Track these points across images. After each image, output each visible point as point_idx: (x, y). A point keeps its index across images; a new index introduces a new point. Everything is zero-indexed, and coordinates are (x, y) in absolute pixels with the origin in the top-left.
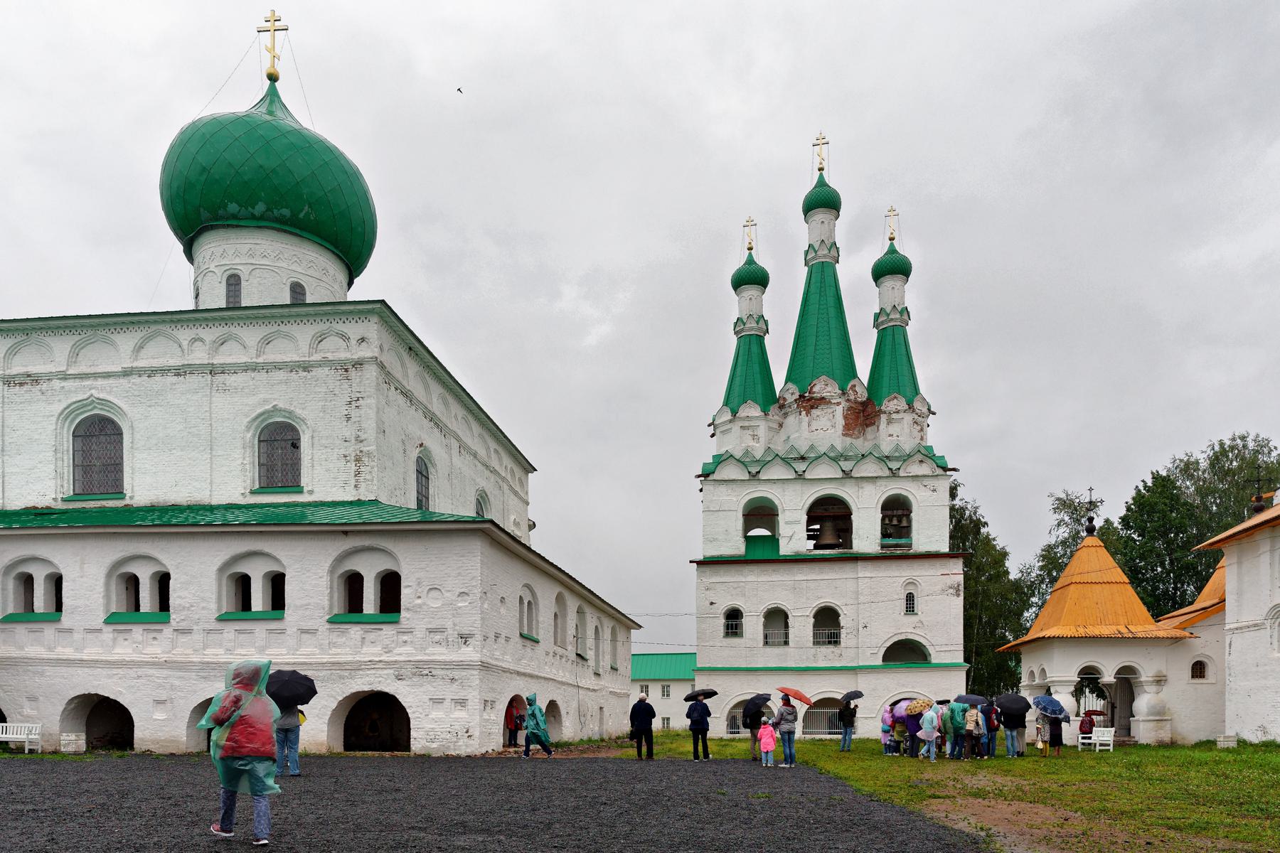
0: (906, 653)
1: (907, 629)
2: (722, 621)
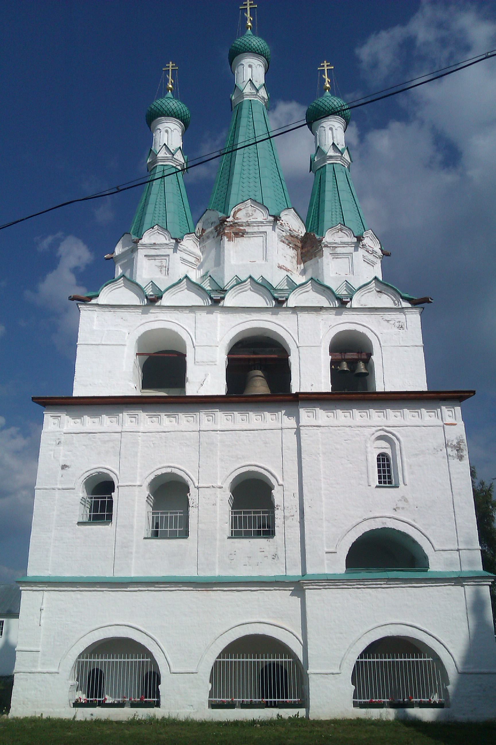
0: (383, 554)
1: (382, 510)
2: (81, 493)
